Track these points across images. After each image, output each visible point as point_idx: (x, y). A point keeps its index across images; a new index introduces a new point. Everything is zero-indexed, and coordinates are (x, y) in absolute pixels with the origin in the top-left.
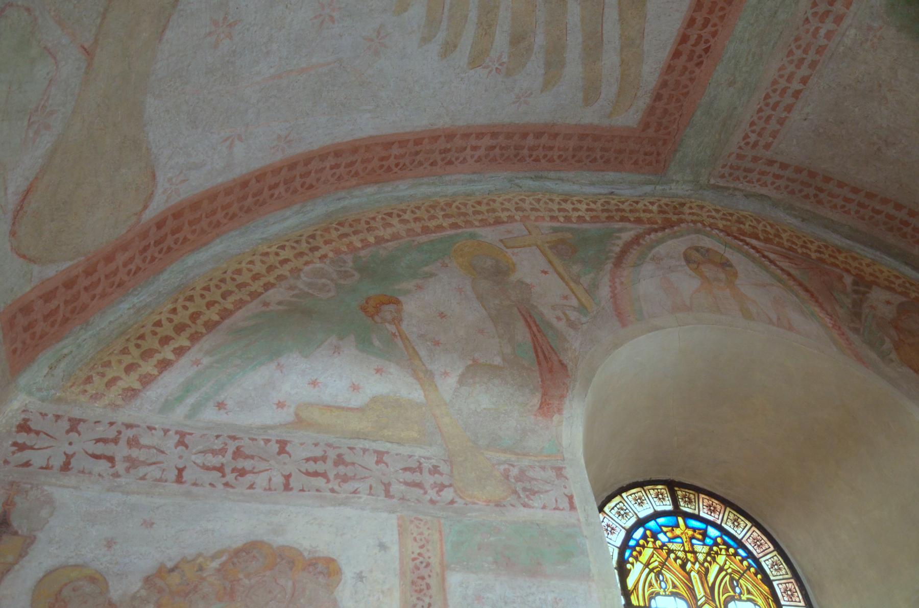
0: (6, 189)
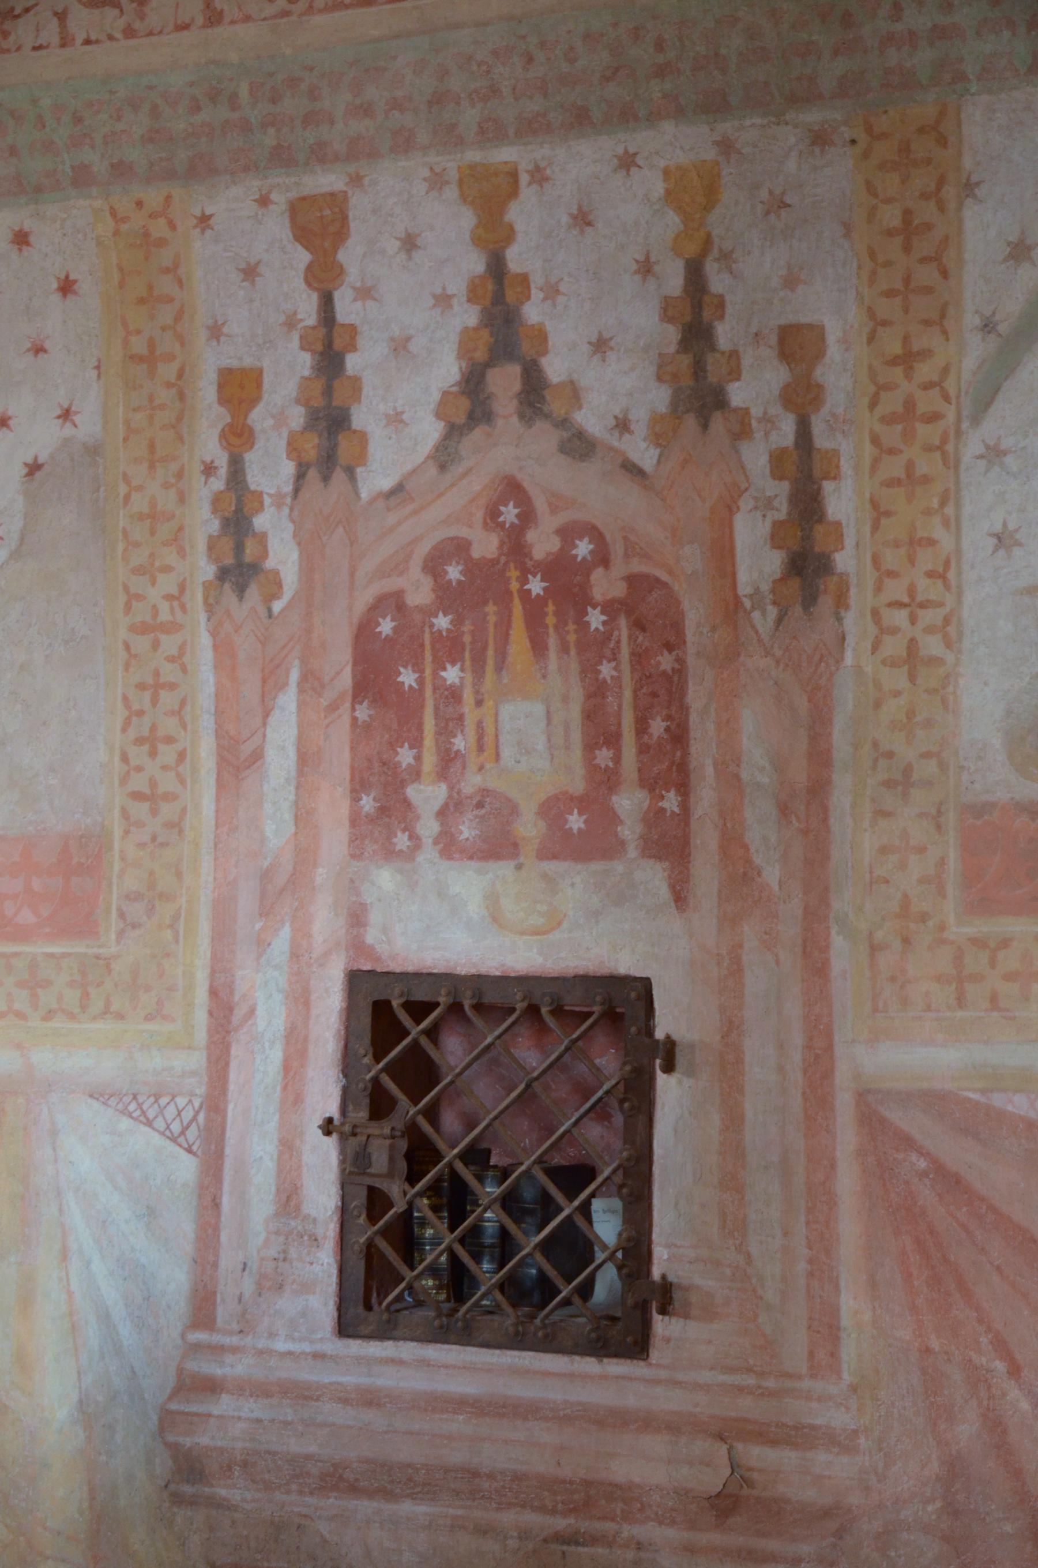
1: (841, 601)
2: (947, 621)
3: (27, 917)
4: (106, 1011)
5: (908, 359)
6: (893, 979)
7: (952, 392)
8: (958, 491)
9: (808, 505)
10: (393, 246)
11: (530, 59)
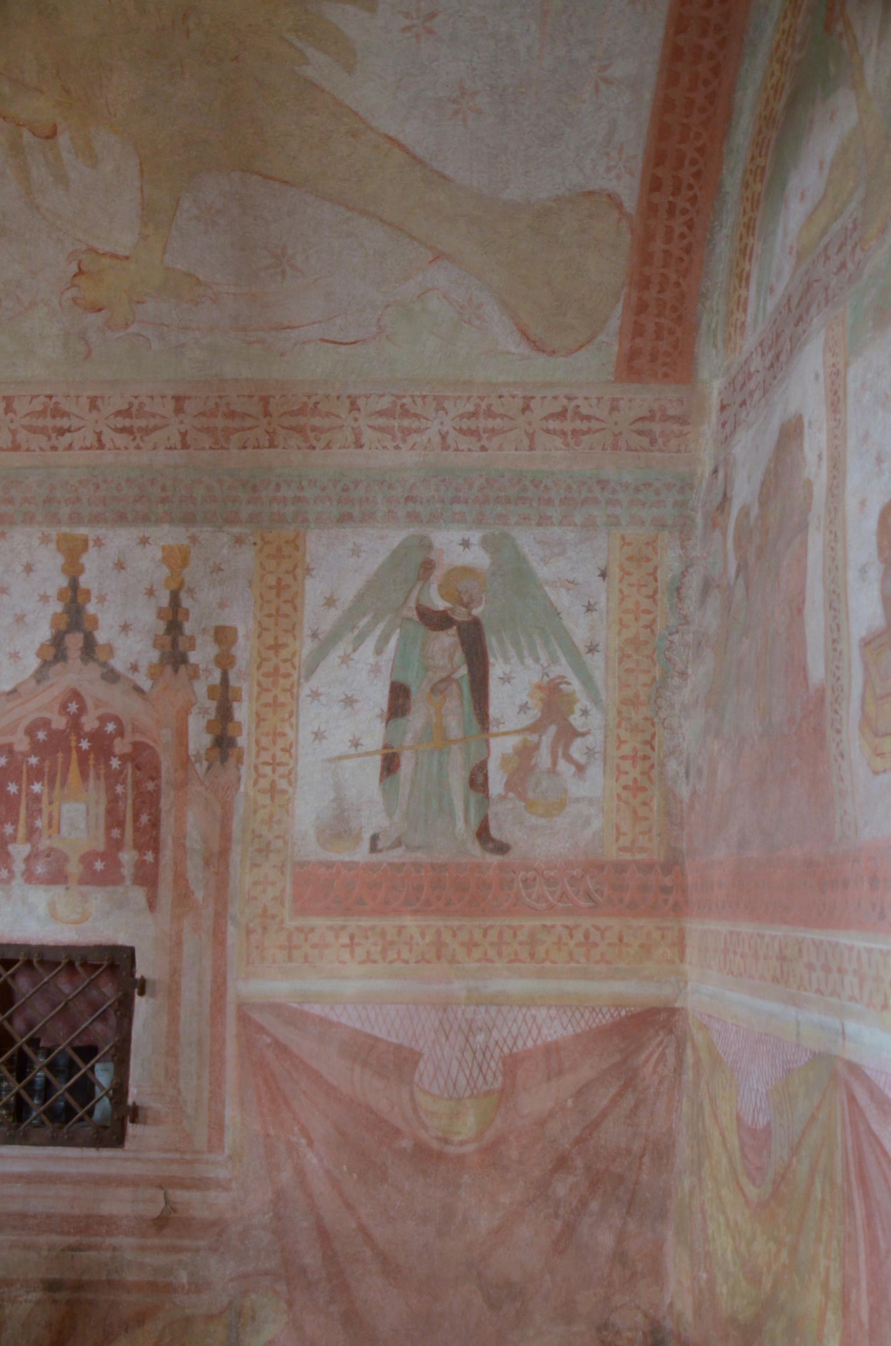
0: (509, 353)
1: (239, 760)
2: (290, 772)
5: (276, 647)
6: (257, 947)
7: (297, 665)
8: (297, 711)
9: (225, 713)
10: (19, 569)
11: (98, 487)
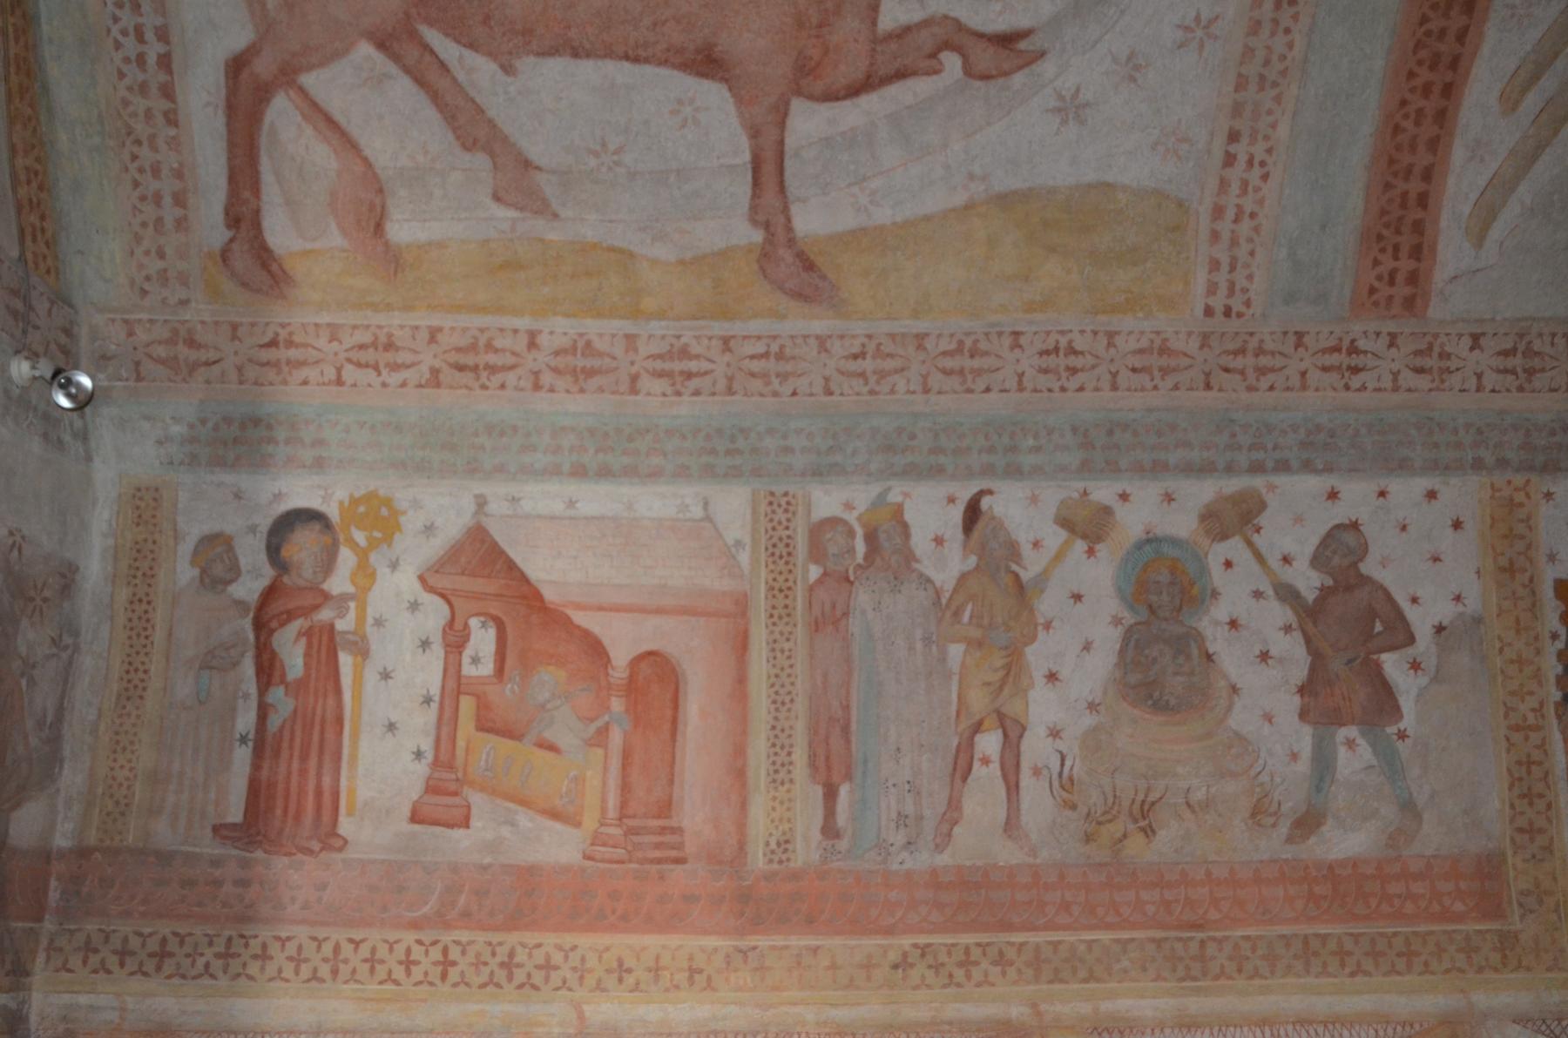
3: (1459, 907)
4: (1519, 967)
